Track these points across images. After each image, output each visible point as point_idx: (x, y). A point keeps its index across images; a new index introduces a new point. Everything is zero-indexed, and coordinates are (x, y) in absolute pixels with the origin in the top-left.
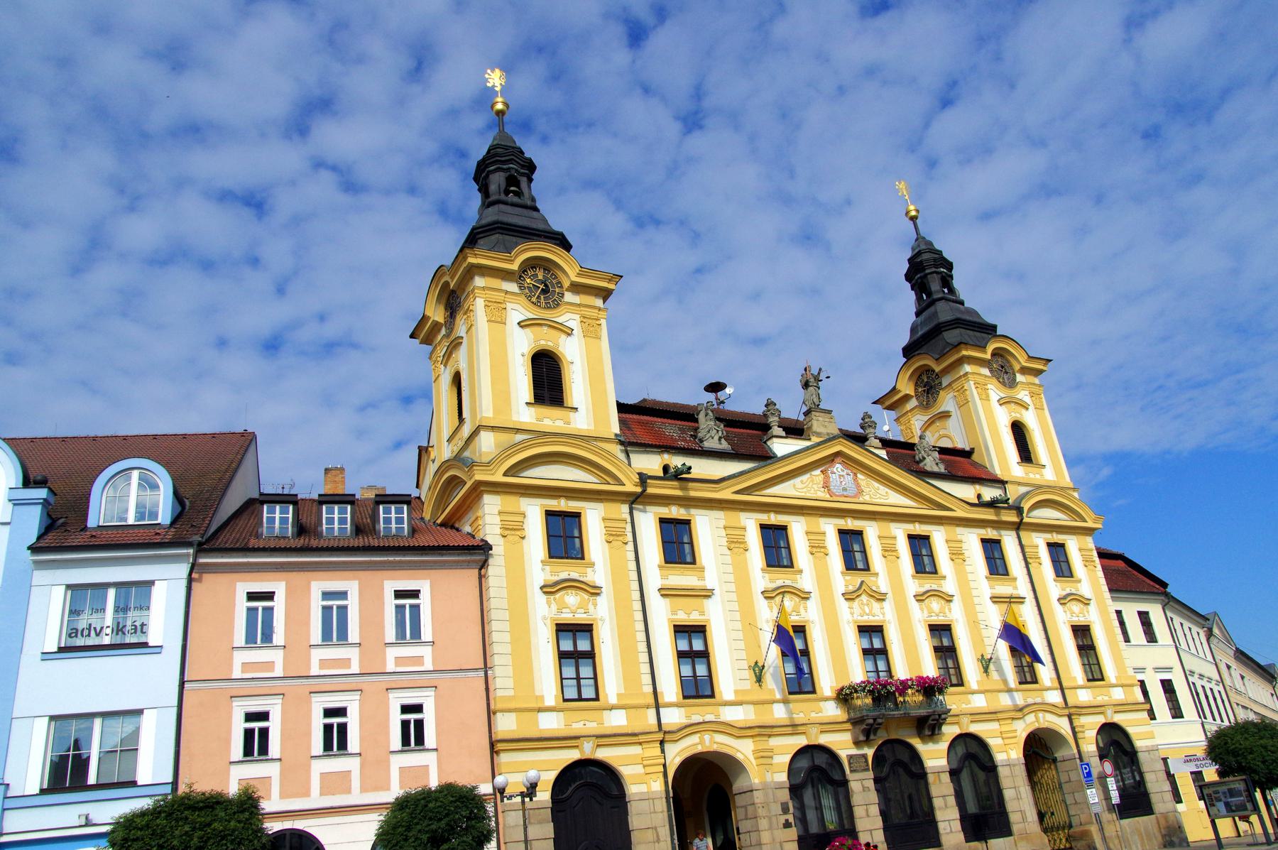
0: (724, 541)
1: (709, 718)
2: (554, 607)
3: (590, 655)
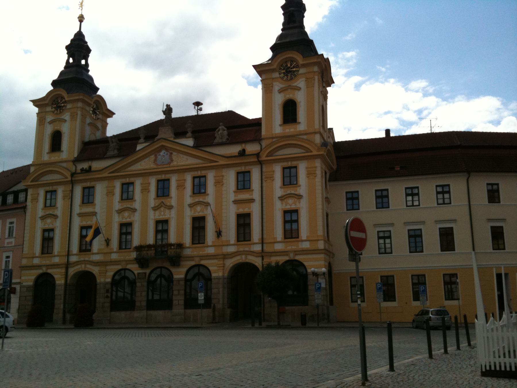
1: (87, 259)
2: (193, 212)
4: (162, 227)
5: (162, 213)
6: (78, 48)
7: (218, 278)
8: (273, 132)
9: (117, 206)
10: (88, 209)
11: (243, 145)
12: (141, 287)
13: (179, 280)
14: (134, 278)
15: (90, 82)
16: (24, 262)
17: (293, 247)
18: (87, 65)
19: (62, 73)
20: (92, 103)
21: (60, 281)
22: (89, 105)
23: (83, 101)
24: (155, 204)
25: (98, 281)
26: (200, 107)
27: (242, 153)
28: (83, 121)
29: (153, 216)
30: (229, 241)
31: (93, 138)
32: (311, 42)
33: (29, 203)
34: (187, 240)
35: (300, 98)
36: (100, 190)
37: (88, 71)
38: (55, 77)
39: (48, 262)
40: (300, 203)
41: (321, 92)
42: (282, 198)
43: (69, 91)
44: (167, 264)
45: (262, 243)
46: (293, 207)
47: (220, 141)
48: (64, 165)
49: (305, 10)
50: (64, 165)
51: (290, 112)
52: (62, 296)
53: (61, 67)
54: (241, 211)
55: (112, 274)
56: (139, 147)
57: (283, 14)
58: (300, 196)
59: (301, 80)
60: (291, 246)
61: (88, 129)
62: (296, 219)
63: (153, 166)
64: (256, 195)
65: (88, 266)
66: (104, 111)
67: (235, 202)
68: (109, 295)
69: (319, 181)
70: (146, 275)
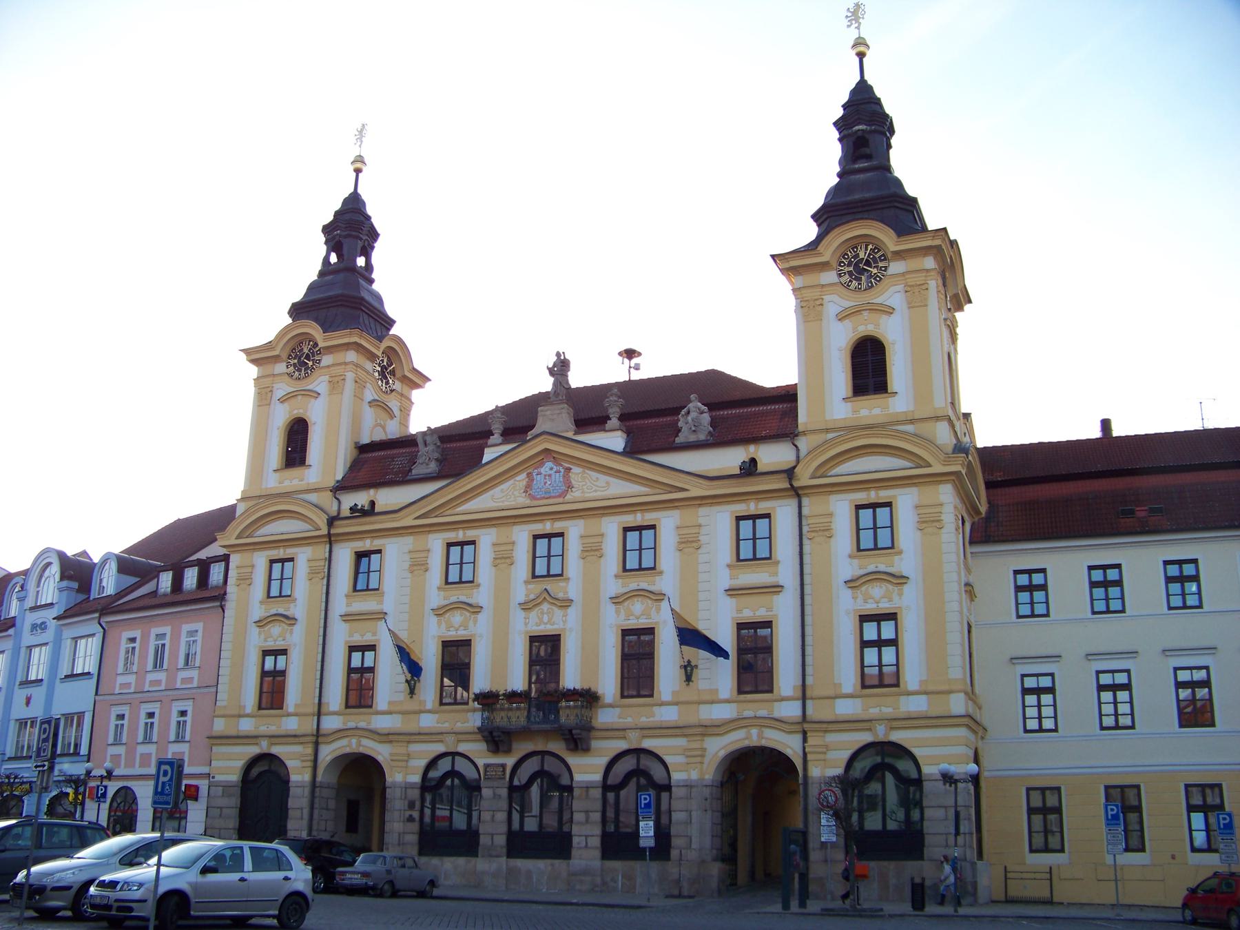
0: (407, 565)
1: (362, 725)
3: (893, 642)
4: (545, 651)
5: (546, 618)
6: (351, 229)
7: (689, 786)
8: (828, 418)
9: (435, 598)
10: (365, 604)
11: (752, 448)
12: (493, 799)
13: (588, 787)
14: (476, 776)
15: (376, 304)
16: (220, 726)
17: (885, 710)
18: (369, 267)
19: (312, 288)
20: (379, 354)
21: (299, 775)
22: (372, 357)
23: (358, 347)
24: (527, 595)
25: (389, 779)
26: (635, 361)
27: (750, 469)
28: (358, 397)
29: (521, 627)
30: (717, 690)
31: (379, 436)
32: (913, 202)
33: (231, 588)
34: (608, 683)
35: (893, 333)
36: (395, 553)
37: (371, 281)
38: (298, 295)
39: (273, 729)
40: (900, 595)
41: (945, 320)
42: (852, 583)
43: (328, 326)
44: (557, 747)
45: (804, 698)
46: (885, 607)
47: (692, 438)
48: (313, 497)
49: (892, 131)
50: (313, 497)
51: (869, 369)
52: (306, 812)
53: (311, 273)
54: (748, 615)
55: (423, 763)
56: (489, 454)
57: (840, 140)
58: (903, 577)
59: (893, 289)
60: (881, 706)
61: (369, 416)
62: (892, 636)
63: (523, 500)
64: (786, 573)
65: (365, 742)
66: (407, 374)
67: (732, 592)
68: (416, 814)
69: (951, 536)
70: (504, 771)
